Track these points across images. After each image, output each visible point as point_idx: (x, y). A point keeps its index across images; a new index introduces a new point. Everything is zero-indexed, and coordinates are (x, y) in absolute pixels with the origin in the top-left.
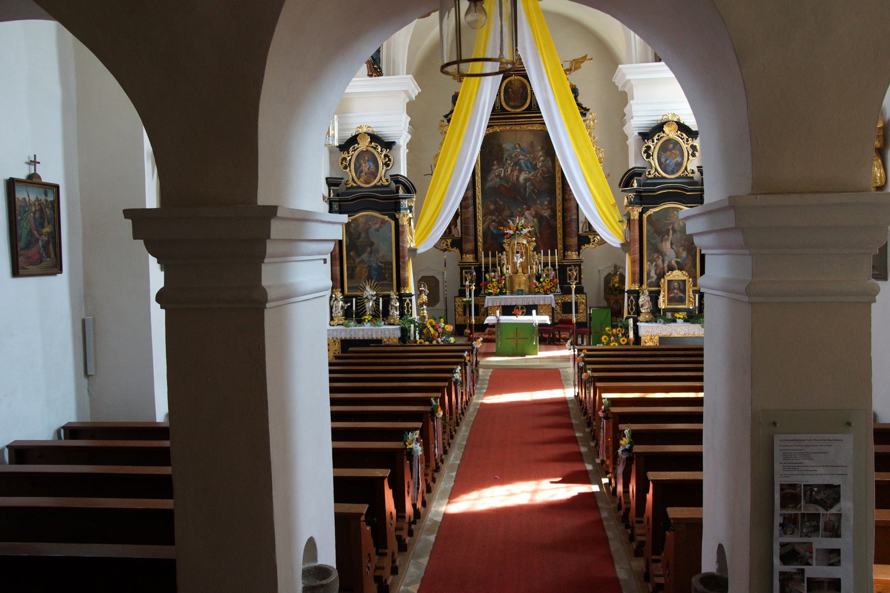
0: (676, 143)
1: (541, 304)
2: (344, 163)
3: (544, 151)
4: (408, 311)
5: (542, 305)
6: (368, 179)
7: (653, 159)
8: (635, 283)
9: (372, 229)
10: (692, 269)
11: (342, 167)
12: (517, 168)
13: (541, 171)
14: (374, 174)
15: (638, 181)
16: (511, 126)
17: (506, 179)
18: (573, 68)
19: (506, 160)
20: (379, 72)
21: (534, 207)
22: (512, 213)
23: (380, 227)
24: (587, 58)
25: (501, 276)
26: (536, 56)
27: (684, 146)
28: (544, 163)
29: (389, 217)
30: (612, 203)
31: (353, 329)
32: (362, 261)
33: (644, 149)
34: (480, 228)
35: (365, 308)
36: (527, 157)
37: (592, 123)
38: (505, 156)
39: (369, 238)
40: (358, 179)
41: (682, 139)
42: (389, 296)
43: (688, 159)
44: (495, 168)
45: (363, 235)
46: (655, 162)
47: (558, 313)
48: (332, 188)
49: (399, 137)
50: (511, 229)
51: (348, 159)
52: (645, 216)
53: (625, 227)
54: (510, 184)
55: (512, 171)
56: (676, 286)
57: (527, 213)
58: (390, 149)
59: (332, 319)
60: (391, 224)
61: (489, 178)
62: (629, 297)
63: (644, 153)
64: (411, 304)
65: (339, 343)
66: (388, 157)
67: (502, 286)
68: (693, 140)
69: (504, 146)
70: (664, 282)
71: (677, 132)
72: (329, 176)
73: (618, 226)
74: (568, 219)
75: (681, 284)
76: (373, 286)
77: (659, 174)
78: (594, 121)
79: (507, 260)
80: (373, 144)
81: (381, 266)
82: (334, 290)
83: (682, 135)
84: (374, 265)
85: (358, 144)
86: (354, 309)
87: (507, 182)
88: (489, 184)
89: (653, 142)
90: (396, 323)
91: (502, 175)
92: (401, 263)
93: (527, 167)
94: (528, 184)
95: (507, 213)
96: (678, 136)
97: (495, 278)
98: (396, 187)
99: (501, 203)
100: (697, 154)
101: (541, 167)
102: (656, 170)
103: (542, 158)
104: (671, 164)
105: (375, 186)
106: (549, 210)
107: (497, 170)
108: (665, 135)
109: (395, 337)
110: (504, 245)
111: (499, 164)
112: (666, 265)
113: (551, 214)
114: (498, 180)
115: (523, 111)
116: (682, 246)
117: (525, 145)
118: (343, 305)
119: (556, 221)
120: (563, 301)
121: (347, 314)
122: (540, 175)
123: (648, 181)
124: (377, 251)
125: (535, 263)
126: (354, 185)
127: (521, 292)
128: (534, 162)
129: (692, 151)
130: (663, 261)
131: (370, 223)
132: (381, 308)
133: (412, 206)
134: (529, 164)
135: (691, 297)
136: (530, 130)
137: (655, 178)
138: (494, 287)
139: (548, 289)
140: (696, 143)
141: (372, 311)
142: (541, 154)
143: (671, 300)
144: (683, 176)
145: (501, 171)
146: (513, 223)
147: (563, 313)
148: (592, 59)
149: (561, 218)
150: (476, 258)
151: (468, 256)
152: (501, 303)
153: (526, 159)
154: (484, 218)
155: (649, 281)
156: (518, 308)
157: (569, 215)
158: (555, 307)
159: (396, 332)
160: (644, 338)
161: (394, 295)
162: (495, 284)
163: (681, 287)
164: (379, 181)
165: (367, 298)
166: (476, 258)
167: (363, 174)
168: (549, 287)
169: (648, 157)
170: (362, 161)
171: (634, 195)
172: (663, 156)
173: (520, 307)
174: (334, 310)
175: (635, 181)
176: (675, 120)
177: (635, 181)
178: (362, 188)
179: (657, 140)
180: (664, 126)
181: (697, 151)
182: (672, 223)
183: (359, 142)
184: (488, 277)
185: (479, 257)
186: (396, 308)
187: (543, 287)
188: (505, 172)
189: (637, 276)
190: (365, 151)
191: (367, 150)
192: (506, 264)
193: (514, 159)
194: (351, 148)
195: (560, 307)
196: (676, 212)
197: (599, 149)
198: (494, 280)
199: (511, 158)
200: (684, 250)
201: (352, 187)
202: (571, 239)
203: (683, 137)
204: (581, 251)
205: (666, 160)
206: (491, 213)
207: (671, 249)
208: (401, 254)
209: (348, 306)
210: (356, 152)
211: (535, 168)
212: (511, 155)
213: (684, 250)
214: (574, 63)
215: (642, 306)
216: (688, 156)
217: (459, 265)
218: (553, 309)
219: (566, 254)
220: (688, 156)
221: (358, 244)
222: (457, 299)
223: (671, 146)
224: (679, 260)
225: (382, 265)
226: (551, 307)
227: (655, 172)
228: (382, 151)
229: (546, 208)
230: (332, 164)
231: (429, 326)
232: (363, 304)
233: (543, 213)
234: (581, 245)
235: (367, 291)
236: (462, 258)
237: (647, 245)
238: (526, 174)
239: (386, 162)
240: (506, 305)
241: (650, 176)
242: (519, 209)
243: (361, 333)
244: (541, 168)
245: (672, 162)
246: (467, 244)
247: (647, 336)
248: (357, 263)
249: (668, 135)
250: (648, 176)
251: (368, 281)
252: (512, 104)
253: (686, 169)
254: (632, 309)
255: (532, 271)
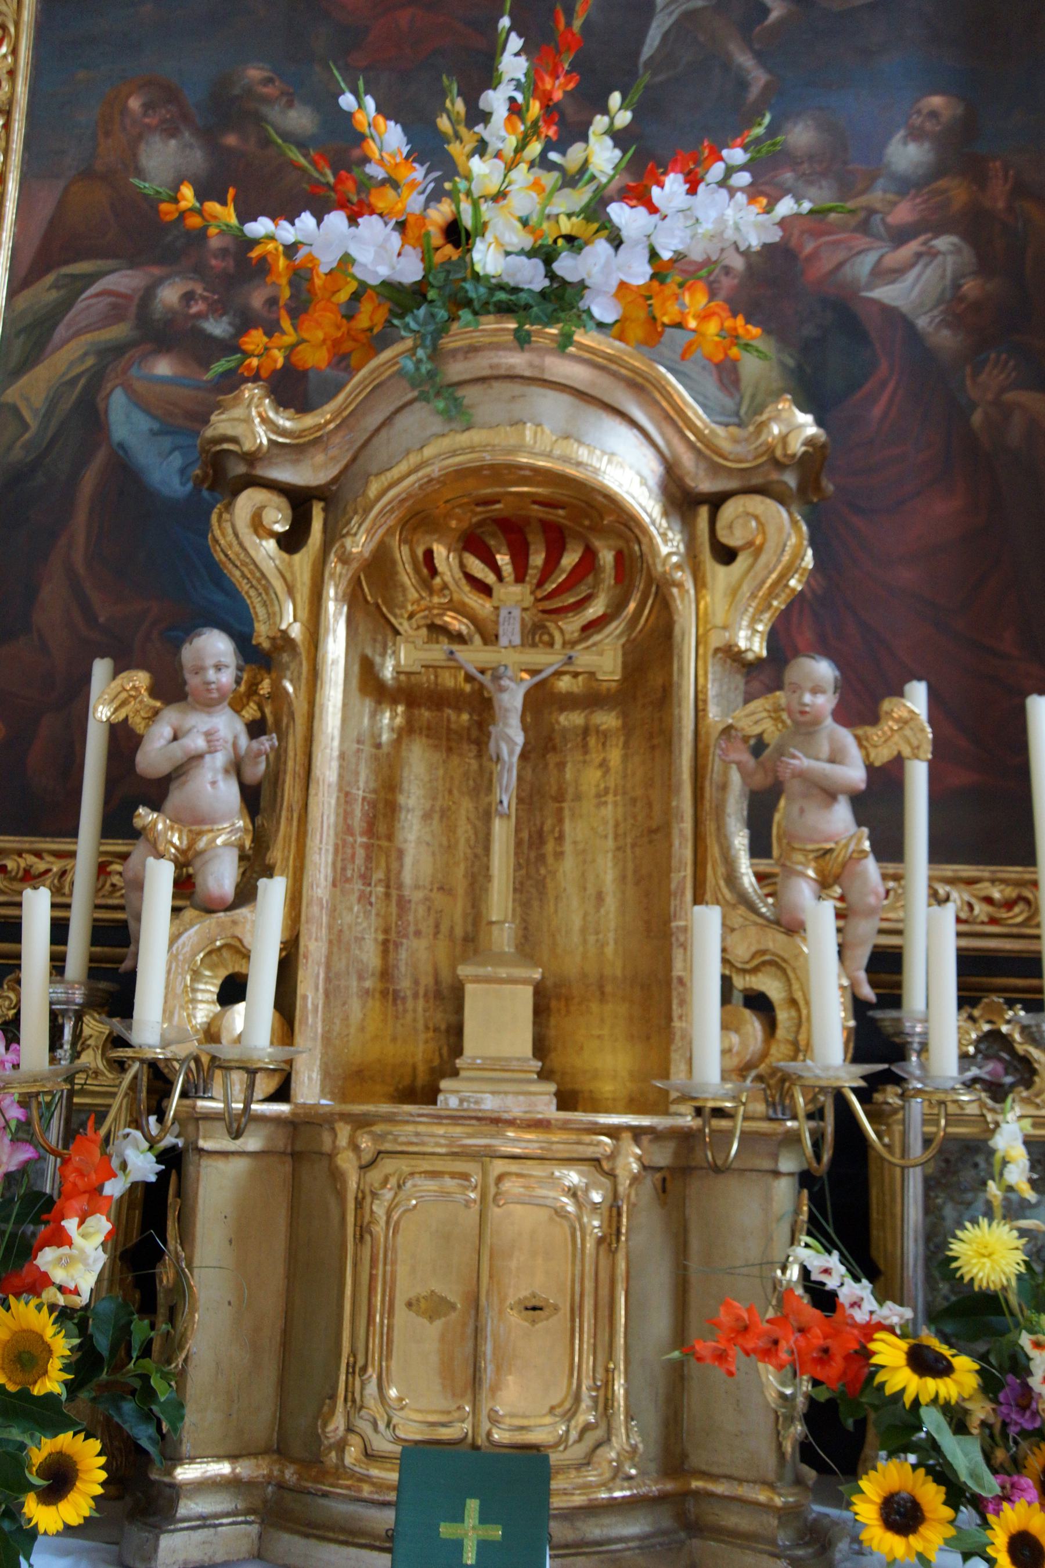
106: (944, 243)
113: (970, 287)
229: (903, 213)
233: (864, 265)
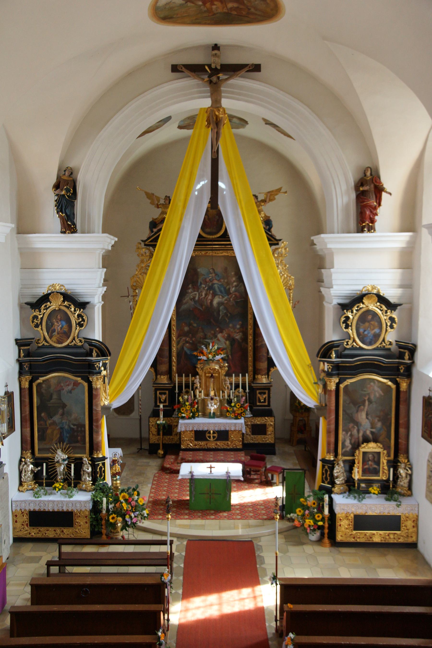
0: (375, 315)
1: (232, 429)
2: (35, 321)
3: (237, 277)
4: (101, 476)
5: (233, 431)
6: (61, 339)
7: (351, 330)
8: (330, 454)
9: (65, 390)
10: (387, 439)
11: (33, 325)
12: (211, 292)
13: (234, 296)
14: (67, 334)
15: (336, 352)
16: (207, 251)
17: (200, 302)
18: (268, 200)
19: (201, 284)
20: (73, 228)
21: (226, 330)
22: (206, 335)
23: (73, 389)
24: (281, 191)
25: (194, 400)
26: (236, 215)
27: (383, 318)
28: (237, 288)
29: (82, 379)
30: (308, 364)
31: (42, 501)
32: (54, 423)
33: (343, 319)
34: (174, 349)
35: (56, 471)
36: (221, 282)
37: (283, 250)
38: (200, 280)
39: (60, 399)
40: (51, 337)
41: (381, 310)
42: (81, 459)
43: (386, 330)
44: (190, 291)
45: (55, 396)
46: (352, 332)
47: (247, 434)
48: (22, 348)
49: (93, 296)
50: (204, 355)
51: (40, 317)
52: (342, 386)
53: (320, 391)
54: (204, 307)
55: (206, 295)
56: (370, 458)
57: (219, 336)
58: (84, 308)
59: (21, 484)
60: (84, 387)
61: (184, 301)
62: (323, 467)
63: (343, 323)
64: (104, 468)
65: (27, 514)
66: (82, 317)
67: (194, 410)
68: (392, 312)
69: (199, 270)
70: (359, 457)
71: (376, 303)
72: (19, 337)
73: (313, 387)
74: (259, 344)
75: (376, 456)
76: (65, 449)
77: (357, 344)
78: (285, 249)
79: (200, 383)
80: (66, 303)
81: (73, 429)
82: (24, 452)
83: (381, 307)
84: (66, 427)
85: (51, 303)
86: (44, 474)
87: (202, 305)
88: (184, 307)
89: (352, 312)
90: (88, 490)
91: (197, 298)
92: (93, 427)
93: (221, 291)
94: (221, 308)
95: (201, 335)
96: (377, 308)
97: (188, 401)
98: (90, 349)
99: (195, 325)
100: (395, 326)
101: (235, 291)
102: (354, 341)
103: (235, 284)
104: (369, 335)
105: (68, 347)
106: (241, 333)
107: (192, 293)
108: (364, 306)
109: (86, 510)
110: (197, 370)
111: (193, 288)
112: (361, 434)
114: (193, 303)
115: (218, 238)
116: (377, 417)
117: (219, 270)
118: (33, 469)
119: (247, 343)
120: (252, 423)
121: (37, 477)
122: (233, 300)
123: (347, 352)
124: (69, 413)
125: (226, 388)
126: (46, 344)
127: (214, 416)
128: (228, 287)
129: (390, 322)
130: (358, 431)
131: (62, 385)
132: (72, 474)
133: (107, 363)
134: (222, 289)
135: (385, 469)
136: (224, 256)
137: (353, 348)
138: (187, 410)
139: (238, 414)
140: (394, 315)
141: (63, 475)
142: (234, 279)
143: (365, 471)
144: (380, 347)
145: (196, 294)
146: (206, 348)
147: (252, 435)
148: (286, 192)
149: (252, 342)
150: (171, 378)
151: (162, 377)
152: (193, 428)
153: (220, 283)
154: (179, 339)
155: (344, 450)
156: (209, 433)
157: (260, 340)
158: (245, 433)
159: (88, 505)
160: (340, 515)
161: (86, 460)
162: (188, 408)
163: (376, 459)
164: (72, 342)
165: (58, 462)
166: (171, 378)
167: (55, 333)
168: (239, 412)
169: (347, 327)
170: (54, 320)
171: (331, 366)
172: (362, 327)
173: (212, 432)
174: (23, 475)
175: (333, 353)
176: (375, 293)
177: (333, 353)
178: (54, 347)
179: (356, 310)
180: (364, 298)
181: (395, 323)
182: (368, 394)
183: (51, 301)
184: (181, 400)
185: (173, 377)
186: (88, 474)
187: (234, 412)
188: (199, 295)
189: (332, 446)
190: (57, 310)
191: (60, 309)
192: (199, 387)
193: (208, 284)
194: (43, 306)
195: (250, 429)
196: (372, 384)
197: (290, 277)
198: (187, 403)
199: (205, 282)
200: (379, 421)
201: (43, 346)
202: (261, 364)
203: (382, 309)
204: (270, 373)
205: (365, 331)
206: (186, 334)
207: (367, 420)
208: (94, 418)
209: (39, 470)
210: (48, 310)
211: (228, 292)
212: (206, 279)
213: (379, 421)
214: (269, 195)
215: (337, 477)
216: (387, 327)
217: (153, 386)
218: (243, 434)
219: (256, 377)
220: (387, 327)
221: (49, 405)
222: (152, 420)
223: (370, 317)
224: (373, 430)
225: (75, 427)
226: (241, 433)
227: (353, 342)
228: (75, 310)
229: (238, 331)
230: (23, 320)
231: (122, 500)
232: (54, 466)
233: (235, 335)
234: (271, 367)
235: (58, 455)
236: (156, 378)
237: (343, 415)
238: (219, 298)
239: (80, 322)
240: (198, 430)
241: (348, 347)
242: (213, 332)
243: (51, 505)
244: (234, 293)
245: (370, 333)
246: (161, 366)
247: (342, 513)
248: (48, 424)
249: (367, 306)
250: (346, 346)
251: (60, 443)
252: (208, 230)
253: (384, 340)
254: (326, 479)
255: (223, 394)
